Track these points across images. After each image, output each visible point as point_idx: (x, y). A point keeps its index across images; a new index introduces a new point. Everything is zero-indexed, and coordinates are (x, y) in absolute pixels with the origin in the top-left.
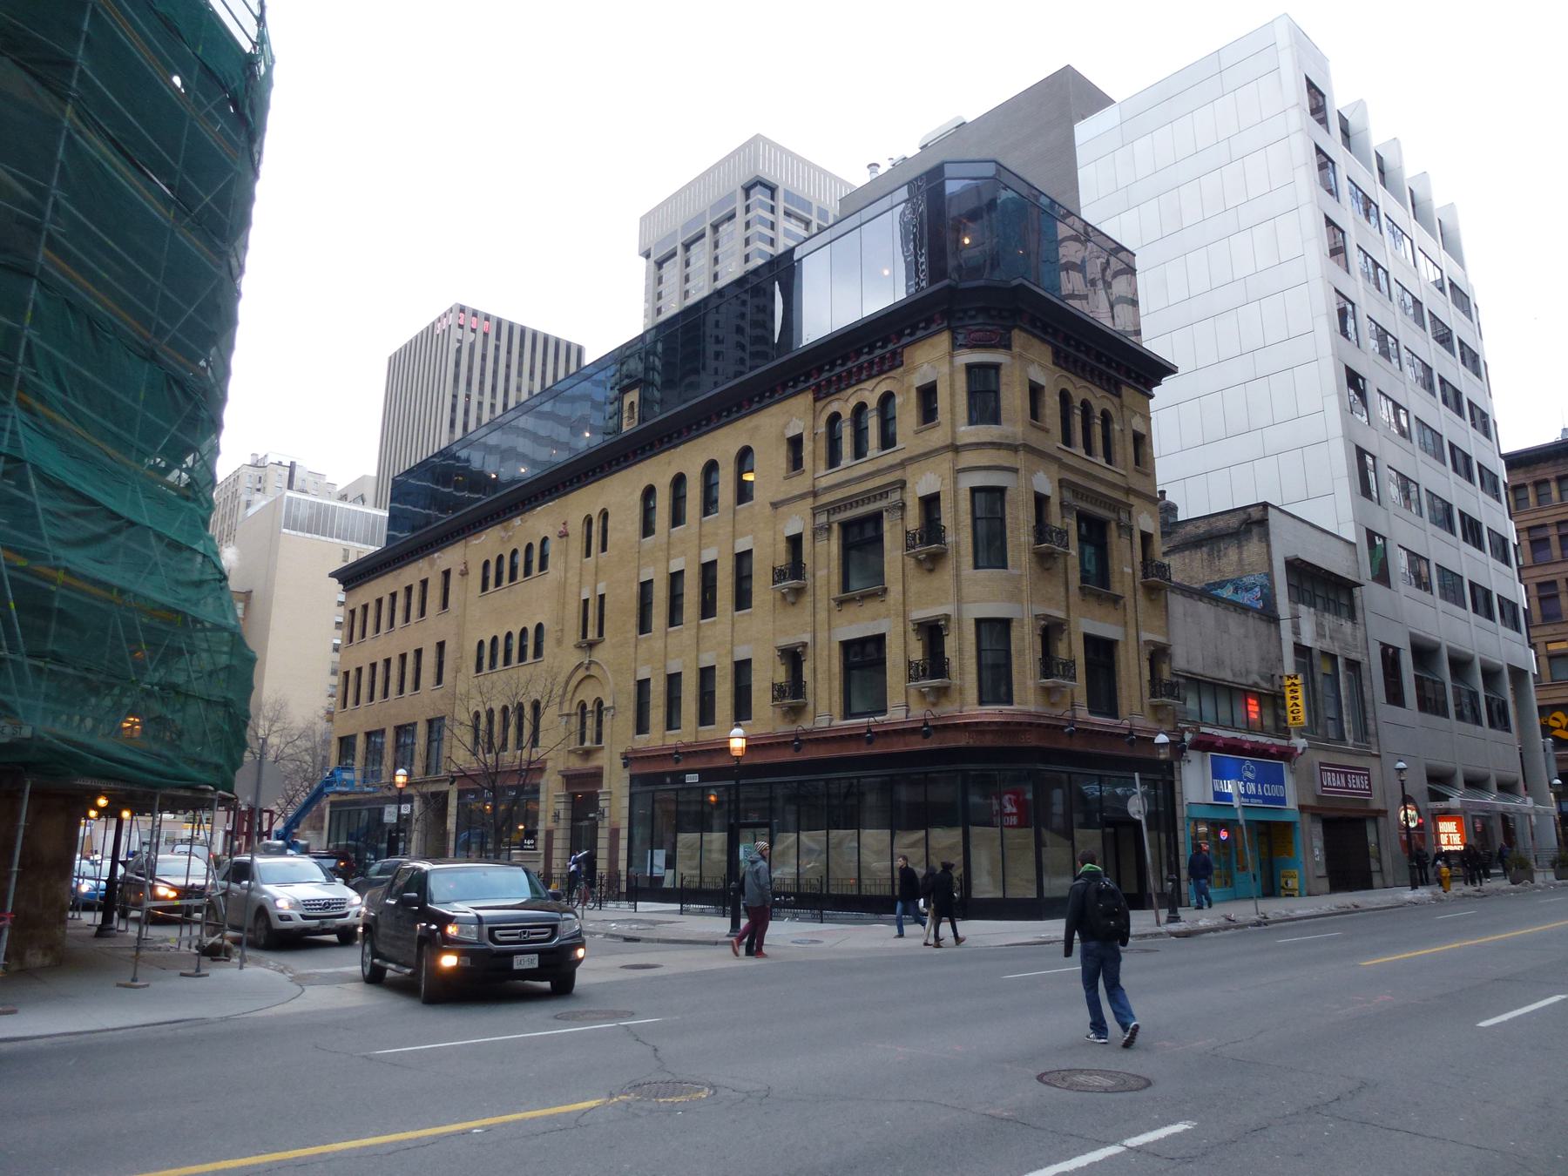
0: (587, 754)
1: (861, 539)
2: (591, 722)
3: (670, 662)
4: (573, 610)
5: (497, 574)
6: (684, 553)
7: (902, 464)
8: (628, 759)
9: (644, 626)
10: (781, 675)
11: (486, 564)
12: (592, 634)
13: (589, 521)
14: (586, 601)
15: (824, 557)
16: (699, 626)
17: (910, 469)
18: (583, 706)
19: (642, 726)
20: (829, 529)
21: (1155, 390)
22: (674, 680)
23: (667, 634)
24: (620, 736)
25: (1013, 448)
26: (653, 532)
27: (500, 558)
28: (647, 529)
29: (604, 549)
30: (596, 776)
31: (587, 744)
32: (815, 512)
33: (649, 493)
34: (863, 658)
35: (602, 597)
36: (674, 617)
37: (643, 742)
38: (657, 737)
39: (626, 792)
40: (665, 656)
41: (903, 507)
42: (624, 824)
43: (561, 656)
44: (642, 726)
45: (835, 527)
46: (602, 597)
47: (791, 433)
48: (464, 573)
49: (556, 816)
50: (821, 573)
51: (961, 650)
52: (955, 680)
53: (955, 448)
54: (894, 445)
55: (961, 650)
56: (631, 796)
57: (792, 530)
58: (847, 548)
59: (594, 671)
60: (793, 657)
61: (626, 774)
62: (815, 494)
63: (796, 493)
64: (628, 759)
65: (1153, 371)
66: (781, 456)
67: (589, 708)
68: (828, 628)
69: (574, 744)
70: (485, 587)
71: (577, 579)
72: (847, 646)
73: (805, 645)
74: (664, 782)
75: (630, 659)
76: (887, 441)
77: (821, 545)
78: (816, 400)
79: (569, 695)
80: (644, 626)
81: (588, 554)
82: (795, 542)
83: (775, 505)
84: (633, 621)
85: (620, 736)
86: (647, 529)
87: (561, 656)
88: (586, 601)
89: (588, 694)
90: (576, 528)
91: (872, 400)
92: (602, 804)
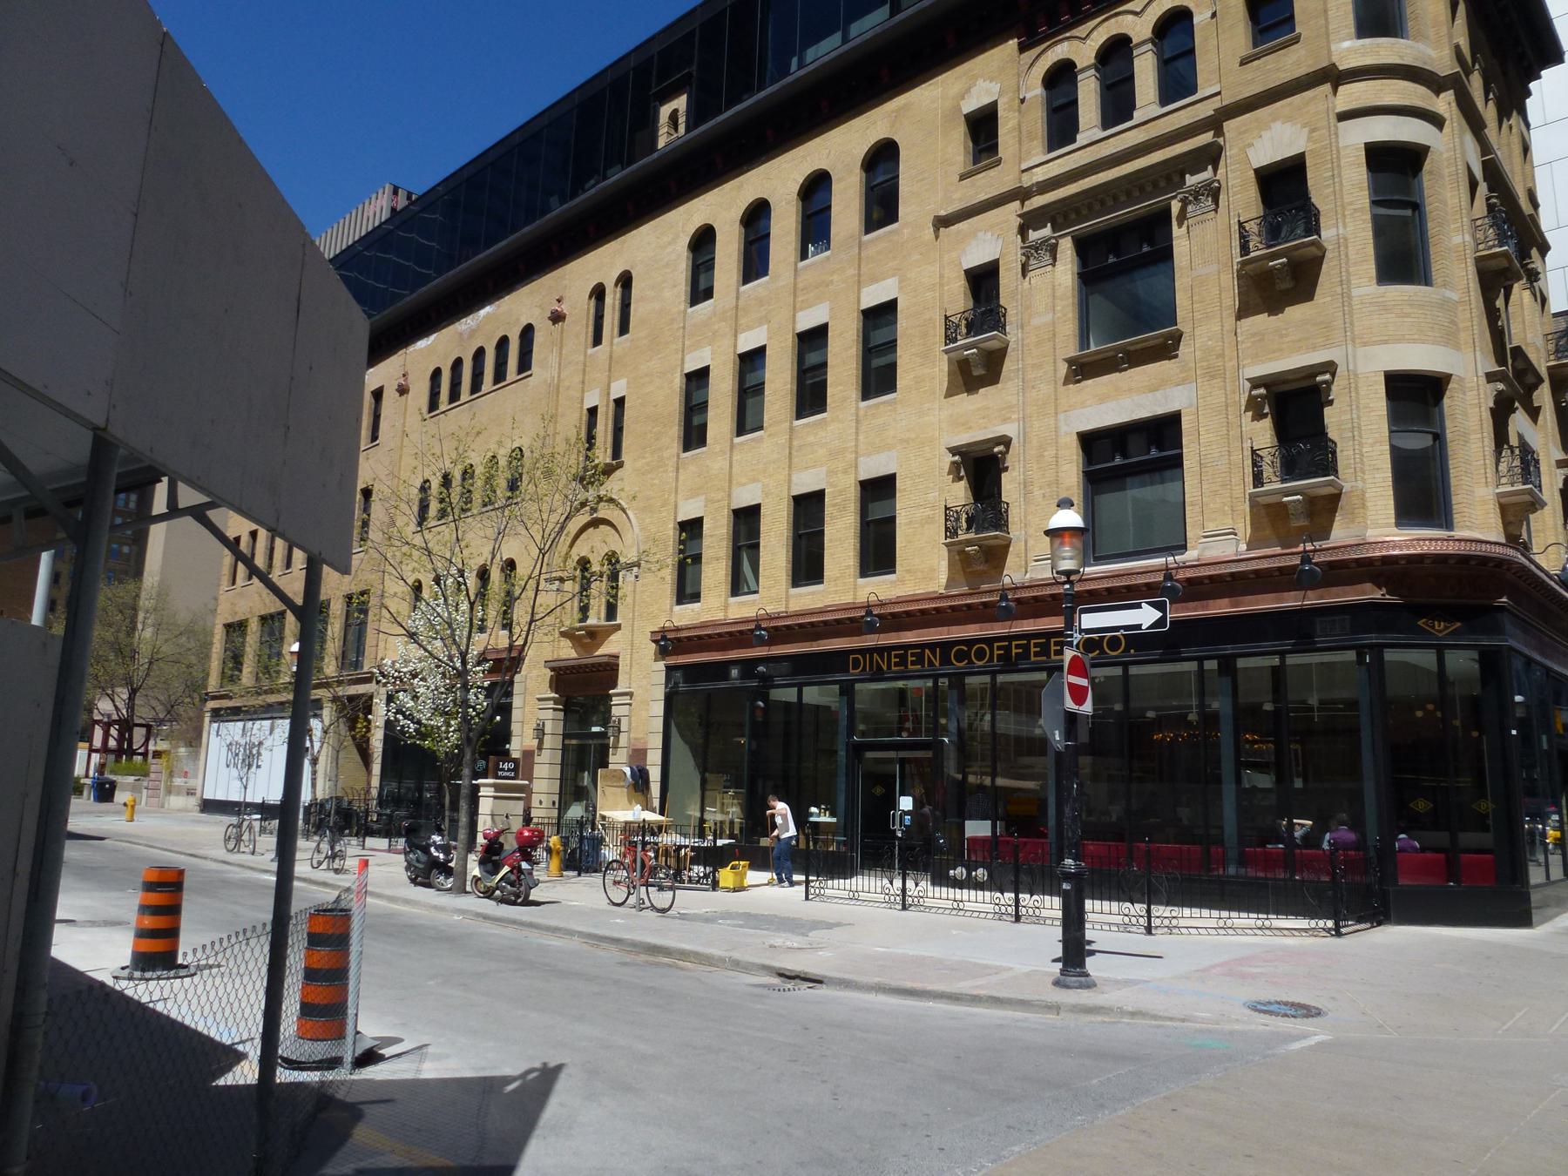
0: (594, 636)
1: (1122, 257)
2: (598, 588)
3: (736, 491)
4: (571, 424)
5: (448, 387)
6: (765, 320)
7: (1215, 123)
8: (668, 643)
9: (694, 436)
10: (959, 494)
11: (437, 374)
12: (603, 455)
13: (599, 293)
14: (593, 412)
15: (1046, 300)
16: (792, 429)
17: (1230, 126)
18: (584, 564)
19: (687, 591)
20: (1053, 251)
21: (1533, 86)
22: (747, 520)
23: (732, 446)
24: (649, 606)
25: (1435, 83)
26: (708, 294)
27: (458, 363)
28: (700, 292)
29: (624, 328)
30: (607, 672)
31: (592, 621)
32: (1029, 222)
33: (703, 241)
34: (1133, 459)
35: (620, 402)
36: (747, 420)
37: (687, 616)
38: (716, 606)
39: (660, 693)
40: (730, 481)
41: (1213, 192)
42: (657, 741)
43: (548, 501)
44: (687, 591)
45: (1066, 247)
46: (620, 402)
47: (971, 105)
48: (403, 390)
49: (540, 732)
50: (1041, 319)
51: (1361, 431)
52: (1347, 477)
53: (1334, 77)
54: (1194, 91)
55: (1361, 431)
56: (670, 700)
57: (976, 257)
58: (1089, 278)
59: (604, 512)
60: (982, 467)
61: (661, 665)
62: (1022, 194)
63: (983, 197)
64: (668, 643)
65: (1547, 51)
66: (957, 144)
67: (595, 568)
68: (1047, 416)
69: (570, 619)
70: (433, 405)
71: (578, 378)
72: (1089, 441)
73: (1006, 441)
74: (726, 676)
75: (661, 490)
76: (1178, 81)
77: (1039, 277)
78: (1023, 48)
79: (565, 540)
80: (694, 436)
81: (597, 340)
82: (983, 280)
83: (942, 222)
84: (675, 431)
85: (649, 606)
86: (700, 292)
87: (548, 501)
88: (593, 412)
89: (594, 546)
90: (579, 307)
91: (1139, 27)
92: (615, 711)
